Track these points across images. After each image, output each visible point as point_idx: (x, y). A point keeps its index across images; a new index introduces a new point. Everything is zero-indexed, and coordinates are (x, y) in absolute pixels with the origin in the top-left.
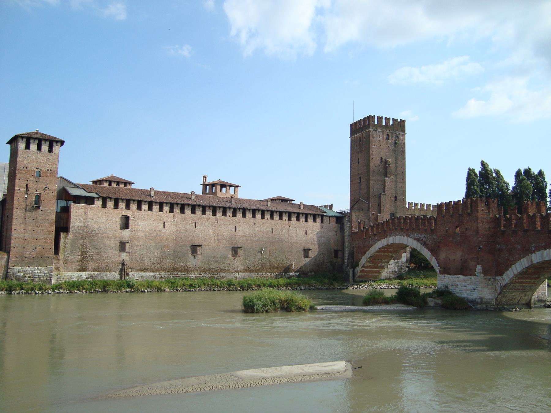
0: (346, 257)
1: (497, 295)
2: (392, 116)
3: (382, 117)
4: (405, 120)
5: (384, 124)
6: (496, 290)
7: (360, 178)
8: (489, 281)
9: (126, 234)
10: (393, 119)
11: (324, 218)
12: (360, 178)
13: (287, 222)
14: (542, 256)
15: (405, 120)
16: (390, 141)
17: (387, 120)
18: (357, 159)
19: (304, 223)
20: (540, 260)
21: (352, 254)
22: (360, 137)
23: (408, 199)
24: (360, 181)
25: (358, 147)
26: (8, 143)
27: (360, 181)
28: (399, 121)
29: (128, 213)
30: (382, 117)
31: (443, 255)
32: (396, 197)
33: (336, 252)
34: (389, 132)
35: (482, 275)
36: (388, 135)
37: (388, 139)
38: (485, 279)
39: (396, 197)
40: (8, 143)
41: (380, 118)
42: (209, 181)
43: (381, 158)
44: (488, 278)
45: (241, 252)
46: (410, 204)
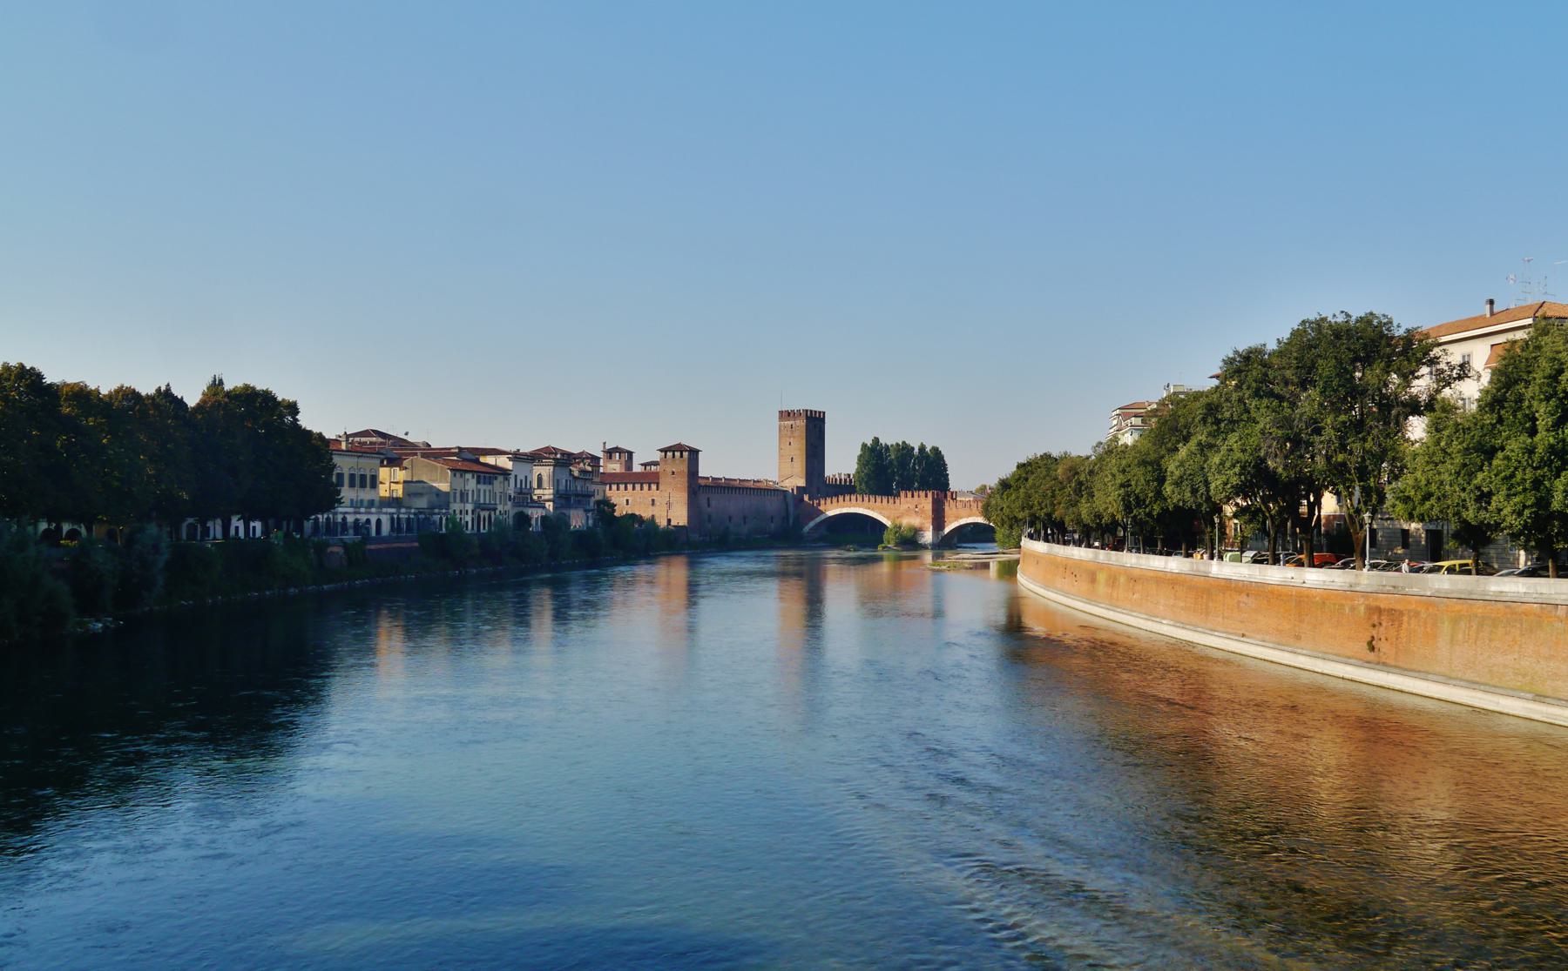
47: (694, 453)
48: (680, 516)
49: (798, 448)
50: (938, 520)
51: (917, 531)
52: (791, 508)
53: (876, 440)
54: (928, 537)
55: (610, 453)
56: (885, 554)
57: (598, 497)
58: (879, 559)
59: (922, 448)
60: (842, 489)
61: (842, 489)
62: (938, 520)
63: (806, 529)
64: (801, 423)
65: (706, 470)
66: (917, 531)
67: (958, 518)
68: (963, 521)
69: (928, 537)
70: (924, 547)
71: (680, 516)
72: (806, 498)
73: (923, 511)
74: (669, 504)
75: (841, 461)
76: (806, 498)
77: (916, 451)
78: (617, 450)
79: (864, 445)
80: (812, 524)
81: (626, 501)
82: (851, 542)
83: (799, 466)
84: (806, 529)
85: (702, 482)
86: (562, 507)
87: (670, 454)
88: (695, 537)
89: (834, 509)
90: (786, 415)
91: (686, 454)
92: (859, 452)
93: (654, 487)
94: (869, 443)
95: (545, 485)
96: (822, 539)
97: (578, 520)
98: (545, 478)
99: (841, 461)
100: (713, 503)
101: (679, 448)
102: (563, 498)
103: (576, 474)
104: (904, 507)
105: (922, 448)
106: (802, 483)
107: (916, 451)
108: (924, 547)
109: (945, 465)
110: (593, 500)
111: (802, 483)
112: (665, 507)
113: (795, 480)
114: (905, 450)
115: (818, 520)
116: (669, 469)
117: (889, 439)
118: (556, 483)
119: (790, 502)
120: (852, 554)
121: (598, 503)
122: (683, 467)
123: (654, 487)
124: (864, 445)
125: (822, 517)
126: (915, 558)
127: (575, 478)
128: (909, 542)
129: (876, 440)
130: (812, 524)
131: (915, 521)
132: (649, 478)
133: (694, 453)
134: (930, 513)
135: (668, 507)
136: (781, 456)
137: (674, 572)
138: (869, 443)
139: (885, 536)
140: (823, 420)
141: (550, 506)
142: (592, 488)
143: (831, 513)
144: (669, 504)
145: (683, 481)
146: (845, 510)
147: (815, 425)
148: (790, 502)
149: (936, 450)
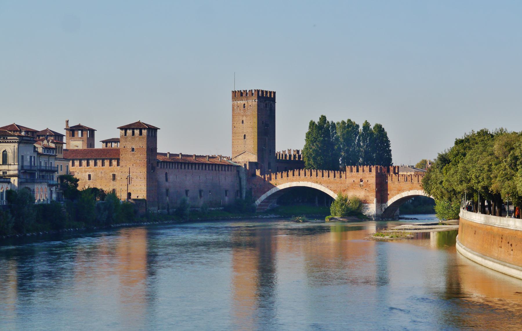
0: (244, 195)
2: (269, 89)
6: (381, 209)
9: (167, 184)
13: (218, 172)
16: (268, 109)
19: (224, 172)
20: (407, 195)
21: (249, 192)
22: (244, 104)
25: (242, 111)
26: (121, 128)
29: (167, 171)
32: (270, 151)
33: (237, 191)
36: (266, 104)
37: (266, 107)
39: (270, 151)
40: (121, 128)
42: (71, 125)
45: (202, 194)
47: (152, 131)
48: (139, 190)
49: (250, 125)
50: (382, 193)
51: (362, 203)
52: (244, 183)
54: (372, 209)
55: (72, 131)
56: (332, 224)
57: (61, 173)
58: (327, 230)
59: (366, 126)
60: (292, 164)
61: (292, 164)
62: (382, 193)
63: (258, 202)
64: (253, 103)
65: (163, 146)
66: (362, 203)
67: (400, 191)
68: (405, 194)
69: (372, 209)
70: (368, 218)
71: (139, 190)
72: (258, 173)
73: (367, 185)
74: (129, 179)
75: (291, 138)
76: (258, 173)
78: (79, 128)
79: (312, 124)
80: (263, 197)
81: (88, 176)
82: (301, 214)
83: (252, 143)
84: (258, 202)
85: (160, 158)
86: (27, 182)
87: (129, 132)
88: (154, 210)
89: (283, 183)
90: (238, 95)
91: (144, 132)
92: (307, 130)
93: (114, 163)
94: (317, 121)
95: (10, 160)
96: (272, 211)
97: (42, 194)
98: (10, 155)
99: (291, 138)
100: (171, 178)
101: (138, 126)
102: (28, 174)
103: (40, 150)
104: (349, 181)
105: (366, 126)
106: (254, 158)
108: (368, 218)
109: (387, 141)
110: (56, 175)
111: (254, 158)
112: (125, 182)
113: (248, 156)
114: (350, 127)
115: (269, 193)
116: (129, 146)
117: (336, 117)
118: (21, 159)
119: (243, 176)
120: (300, 225)
121: (62, 178)
122: (141, 143)
123: (114, 163)
124: (312, 124)
125: (273, 191)
126: (360, 229)
127: (39, 154)
128: (355, 213)
130: (263, 197)
131: (361, 194)
132: (110, 154)
133: (152, 131)
135: (130, 183)
136: (234, 133)
137: (133, 242)
138: (317, 121)
139: (332, 208)
140: (273, 100)
141: (15, 181)
142: (55, 163)
143: (281, 187)
144: (129, 179)
145: (142, 157)
146: (295, 184)
147: (266, 103)
148: (243, 176)
149: (379, 128)
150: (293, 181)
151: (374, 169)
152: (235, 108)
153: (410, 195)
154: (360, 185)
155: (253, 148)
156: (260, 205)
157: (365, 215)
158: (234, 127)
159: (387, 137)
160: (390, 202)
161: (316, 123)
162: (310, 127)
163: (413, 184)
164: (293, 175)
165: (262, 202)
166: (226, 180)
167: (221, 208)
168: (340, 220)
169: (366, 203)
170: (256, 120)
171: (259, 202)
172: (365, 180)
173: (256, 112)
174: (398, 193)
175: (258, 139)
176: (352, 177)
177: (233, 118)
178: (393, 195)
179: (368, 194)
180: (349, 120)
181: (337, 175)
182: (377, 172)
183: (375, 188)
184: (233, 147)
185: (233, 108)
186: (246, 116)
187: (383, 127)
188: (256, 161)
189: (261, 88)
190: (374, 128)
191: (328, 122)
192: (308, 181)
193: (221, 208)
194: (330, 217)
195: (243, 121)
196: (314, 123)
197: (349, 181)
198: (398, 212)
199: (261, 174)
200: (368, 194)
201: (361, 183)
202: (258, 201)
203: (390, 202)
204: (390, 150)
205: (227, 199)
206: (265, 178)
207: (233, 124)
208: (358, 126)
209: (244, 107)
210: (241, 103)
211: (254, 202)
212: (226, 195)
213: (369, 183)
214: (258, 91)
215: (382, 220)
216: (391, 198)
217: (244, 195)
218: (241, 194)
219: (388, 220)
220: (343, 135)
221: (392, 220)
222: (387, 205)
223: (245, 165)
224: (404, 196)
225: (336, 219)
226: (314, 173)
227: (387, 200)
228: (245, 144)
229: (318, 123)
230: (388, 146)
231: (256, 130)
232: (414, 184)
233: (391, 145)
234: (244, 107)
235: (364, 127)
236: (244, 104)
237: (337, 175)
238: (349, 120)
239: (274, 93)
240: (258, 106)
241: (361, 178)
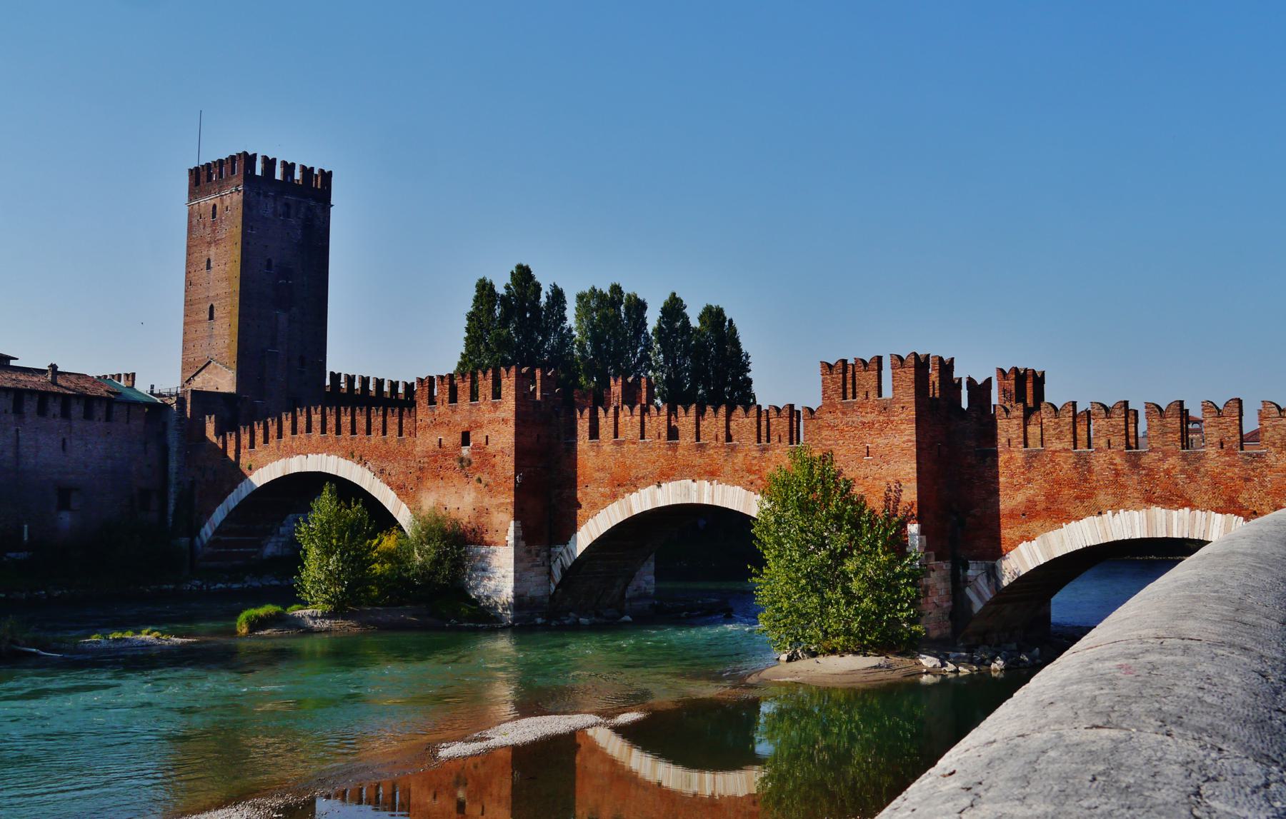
0: (171, 508)
1: (553, 587)
3: (274, 160)
4: (330, 173)
5: (278, 175)
6: (550, 573)
7: (212, 307)
8: (537, 555)
10: (303, 168)
11: (115, 408)
12: (212, 307)
14: (653, 499)
15: (330, 173)
17: (288, 168)
18: (205, 260)
22: (215, 206)
23: (332, 365)
24: (211, 317)
25: (208, 230)
27: (211, 317)
28: (316, 172)
30: (274, 160)
31: (429, 501)
34: (291, 199)
35: (523, 543)
36: (287, 205)
38: (529, 552)
41: (269, 164)
43: (269, 261)
44: (534, 548)
46: (335, 377)
50: (545, 498)
51: (459, 544)
52: (173, 465)
53: (523, 276)
54: (500, 576)
59: (673, 309)
62: (545, 498)
63: (207, 531)
64: (231, 199)
66: (459, 544)
67: (623, 484)
69: (500, 576)
70: (483, 619)
73: (485, 457)
77: (652, 319)
79: (485, 289)
80: (219, 515)
84: (207, 531)
92: (469, 307)
105: (673, 309)
106: (223, 380)
107: (652, 319)
111: (223, 380)
115: (233, 500)
124: (485, 289)
125: (241, 492)
129: (523, 276)
130: (219, 515)
131: (458, 501)
134: (507, 465)
136: (188, 303)
143: (260, 478)
146: (296, 465)
150: (291, 453)
151: (509, 384)
152: (195, 221)
153: (662, 503)
154: (461, 460)
155: (229, 346)
156: (212, 543)
157: (476, 602)
158: (189, 283)
159: (736, 343)
160: (584, 538)
161: (500, 290)
162: (476, 300)
163: (674, 448)
164: (294, 431)
165: (217, 532)
166: (89, 450)
167: (23, 555)
168: (310, 631)
169: (482, 543)
170: (237, 252)
171: (210, 533)
172: (476, 437)
173: (240, 227)
174: (614, 497)
175: (242, 315)
176: (436, 425)
177: (189, 254)
178: (596, 507)
179: (487, 501)
180: (616, 289)
181: (393, 421)
182: (523, 398)
183: (510, 470)
184: (185, 349)
185: (190, 222)
186: (216, 242)
187: (728, 315)
188: (233, 389)
189: (261, 149)
190: (701, 318)
191: (538, 288)
192: (329, 450)
193: (23, 555)
194: (268, 609)
195: (209, 261)
196: (491, 286)
197: (425, 441)
198: (646, 579)
199: (220, 432)
200: (487, 501)
201: (465, 451)
202: (207, 526)
203: (584, 538)
204: (750, 382)
205: (66, 518)
206: (225, 443)
207: (188, 273)
208: (638, 307)
209: (214, 216)
210: (207, 201)
211: (194, 531)
212: (64, 504)
213: (490, 449)
214: (249, 160)
215: (546, 627)
216: (584, 522)
217: (171, 508)
218: (165, 505)
219: (576, 629)
220: (593, 327)
221: (596, 628)
222: (569, 552)
223: (181, 401)
224: (636, 511)
225: (297, 624)
226: (377, 422)
227: (573, 529)
228: (211, 336)
229: (507, 287)
230: (745, 368)
231: (236, 286)
232: (680, 451)
233: (751, 366)
234: (214, 216)
235: (664, 311)
236: (215, 206)
237: (393, 421)
238: (616, 289)
239: (326, 177)
240: (247, 204)
241: (465, 425)
